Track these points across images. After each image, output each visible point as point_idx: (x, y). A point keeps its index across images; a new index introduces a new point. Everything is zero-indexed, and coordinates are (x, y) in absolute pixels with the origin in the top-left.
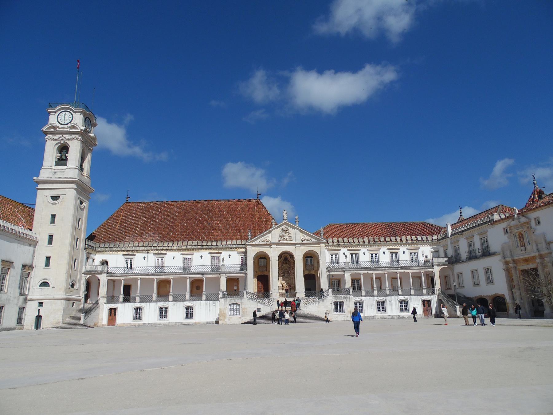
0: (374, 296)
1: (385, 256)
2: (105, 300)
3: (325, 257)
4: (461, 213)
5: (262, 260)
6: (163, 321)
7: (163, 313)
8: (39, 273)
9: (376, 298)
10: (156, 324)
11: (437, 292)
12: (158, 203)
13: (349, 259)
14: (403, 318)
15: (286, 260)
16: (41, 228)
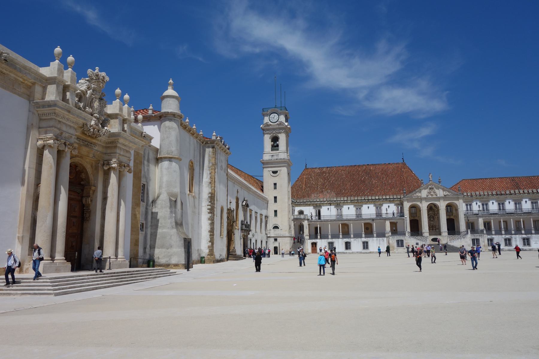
0: (502, 234)
1: (510, 206)
2: (308, 237)
3: (462, 207)
5: (415, 211)
6: (348, 251)
7: (348, 246)
8: (273, 221)
9: (504, 236)
10: (344, 253)
12: (329, 169)
13: (481, 208)
14: (526, 250)
16: (269, 193)
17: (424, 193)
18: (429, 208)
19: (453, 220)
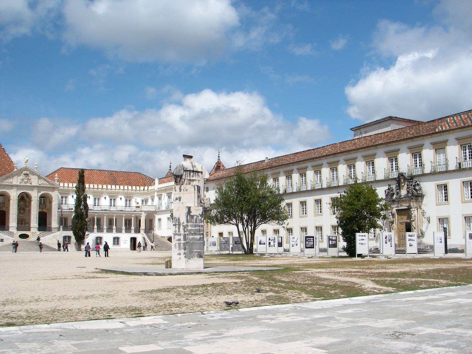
4: (170, 167)
11: (142, 232)
15: (24, 200)
17: (16, 181)
18: (20, 197)
19: (46, 213)
